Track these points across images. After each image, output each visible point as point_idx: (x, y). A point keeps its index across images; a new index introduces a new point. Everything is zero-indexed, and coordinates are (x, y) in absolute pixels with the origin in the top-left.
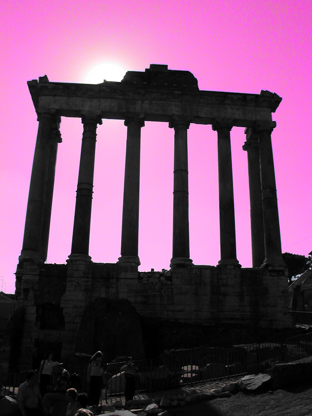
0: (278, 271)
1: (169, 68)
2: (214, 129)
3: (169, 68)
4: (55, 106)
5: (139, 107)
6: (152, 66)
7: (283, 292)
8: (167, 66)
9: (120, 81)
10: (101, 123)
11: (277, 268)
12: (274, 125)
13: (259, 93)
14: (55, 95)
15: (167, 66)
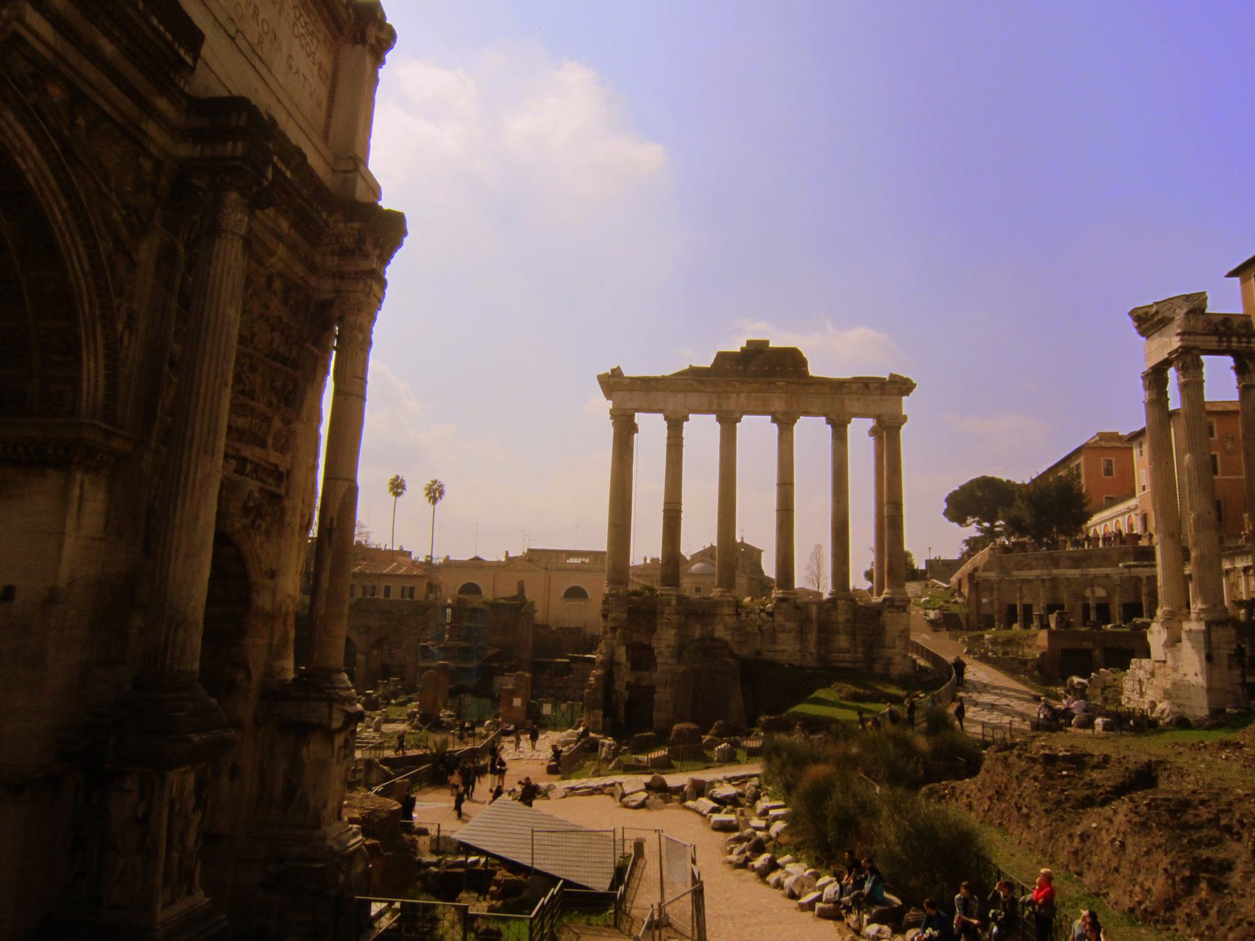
0: (898, 607)
1: (771, 345)
2: (828, 423)
3: (771, 345)
4: (631, 405)
5: (732, 403)
6: (749, 342)
7: (903, 632)
8: (767, 342)
9: (709, 366)
10: (687, 419)
11: (897, 604)
12: (905, 419)
13: (887, 377)
14: (632, 390)
15: (767, 342)
